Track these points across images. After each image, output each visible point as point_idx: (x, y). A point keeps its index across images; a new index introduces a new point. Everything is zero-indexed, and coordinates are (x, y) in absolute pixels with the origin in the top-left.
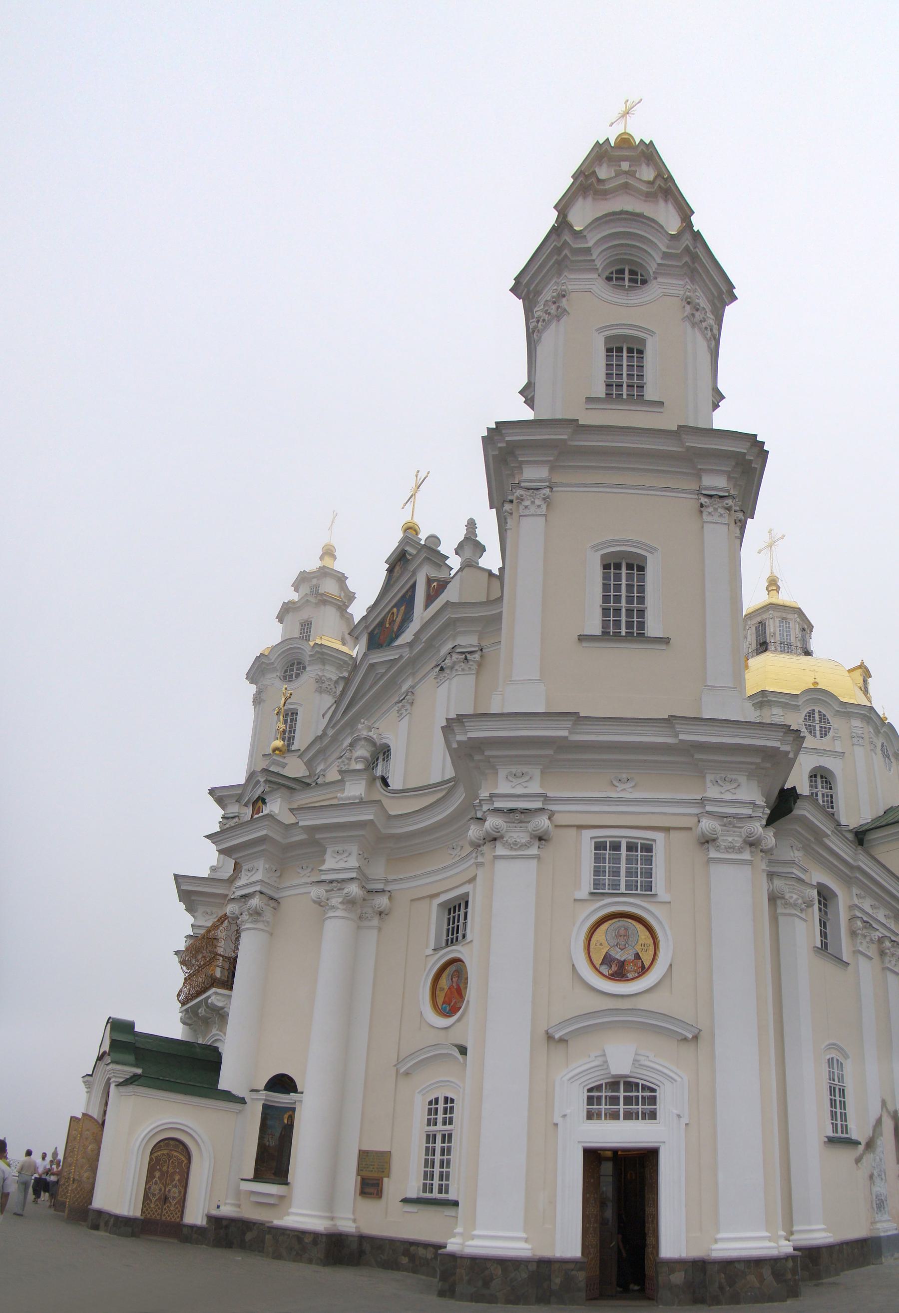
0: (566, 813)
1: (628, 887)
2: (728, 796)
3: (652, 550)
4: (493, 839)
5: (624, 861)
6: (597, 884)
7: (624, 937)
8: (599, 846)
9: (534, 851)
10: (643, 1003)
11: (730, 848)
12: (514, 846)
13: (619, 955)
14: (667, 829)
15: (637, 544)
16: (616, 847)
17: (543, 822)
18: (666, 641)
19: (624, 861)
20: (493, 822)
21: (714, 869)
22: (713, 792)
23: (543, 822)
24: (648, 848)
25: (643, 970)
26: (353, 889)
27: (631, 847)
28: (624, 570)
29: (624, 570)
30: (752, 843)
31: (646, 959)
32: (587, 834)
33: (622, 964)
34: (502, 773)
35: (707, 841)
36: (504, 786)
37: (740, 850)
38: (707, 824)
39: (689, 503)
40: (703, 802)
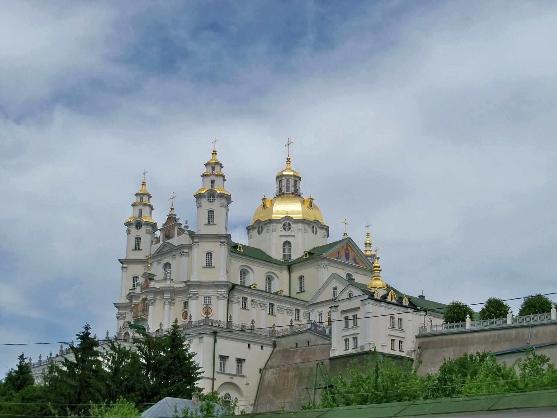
4: (191, 297)
5: (208, 300)
17: (197, 295)
19: (208, 300)
20: (191, 295)
23: (197, 295)
26: (170, 300)
28: (209, 255)
29: (209, 255)
35: (218, 297)
36: (193, 291)
39: (219, 243)
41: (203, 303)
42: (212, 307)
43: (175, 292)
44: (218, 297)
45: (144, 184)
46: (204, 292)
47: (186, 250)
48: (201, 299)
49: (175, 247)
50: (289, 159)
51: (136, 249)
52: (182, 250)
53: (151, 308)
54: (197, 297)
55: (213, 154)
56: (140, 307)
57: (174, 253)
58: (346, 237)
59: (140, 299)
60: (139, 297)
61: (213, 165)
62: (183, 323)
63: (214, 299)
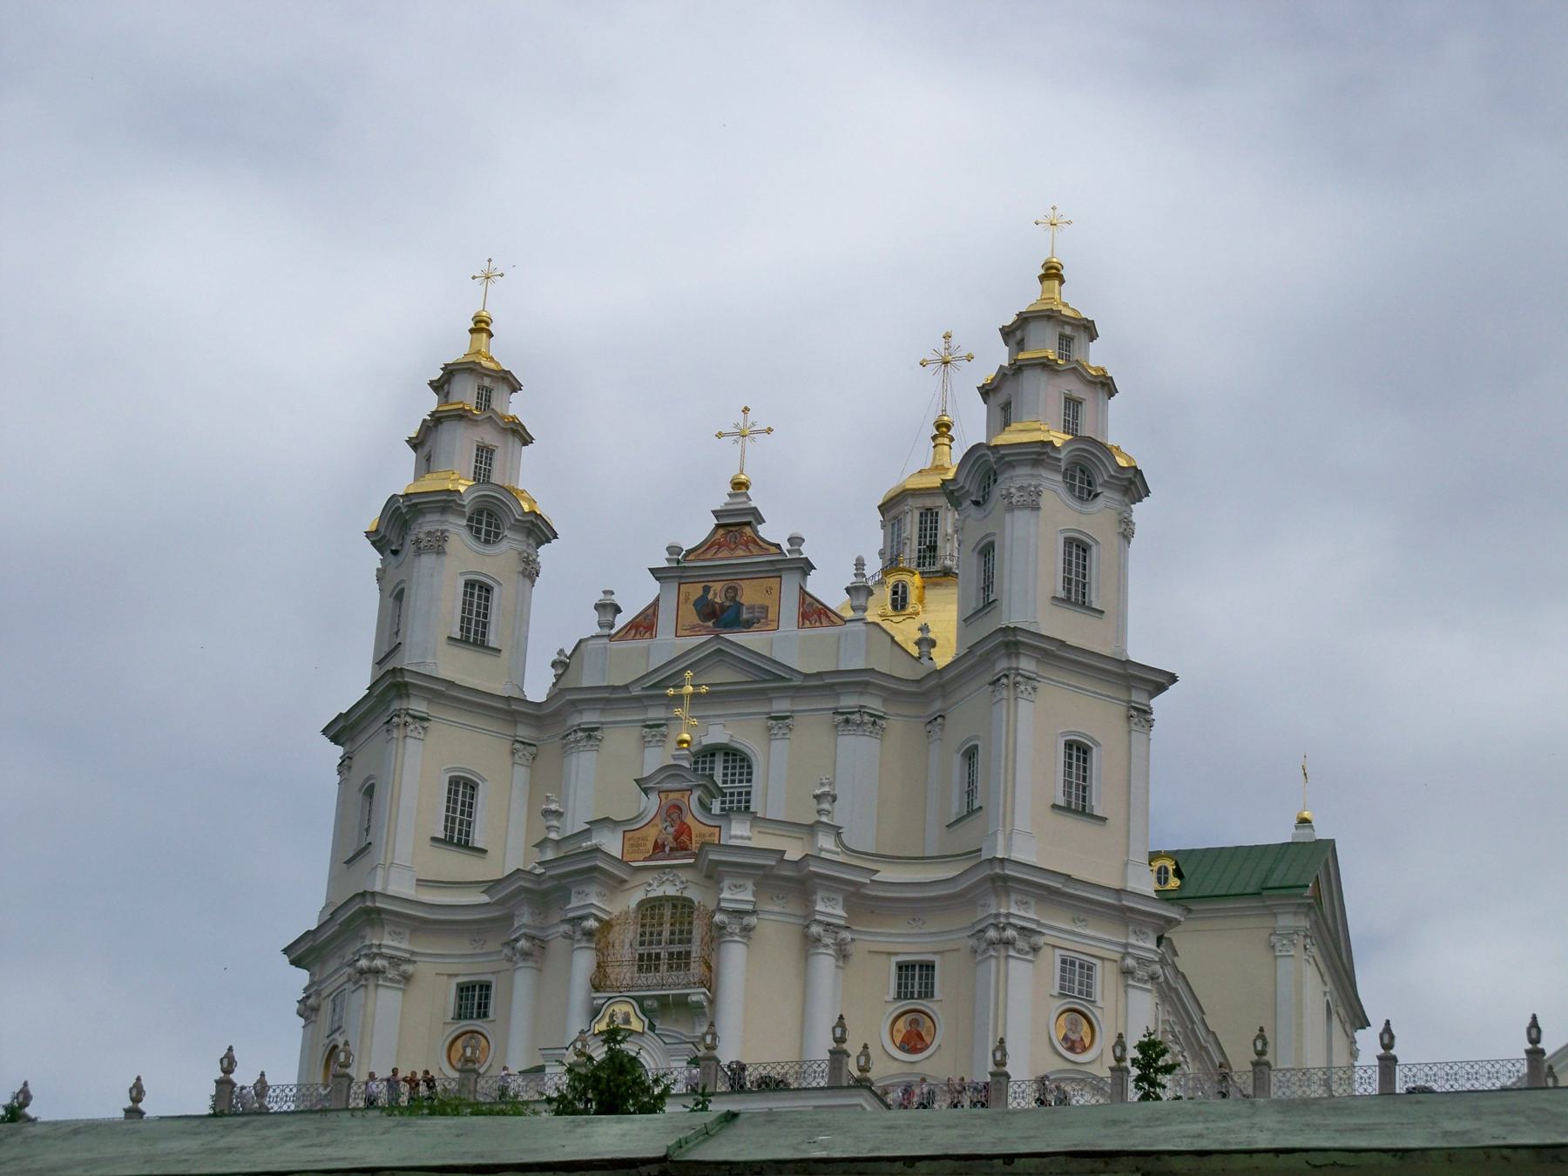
0: (1049, 938)
1: (1080, 992)
2: (1141, 944)
3: (1098, 744)
4: (1008, 943)
6: (1062, 988)
7: (1074, 1026)
8: (1064, 961)
9: (1029, 957)
10: (1088, 1069)
11: (1139, 980)
12: (1019, 951)
13: (1074, 1037)
14: (1102, 959)
15: (1084, 736)
16: (1073, 964)
18: (1104, 819)
19: (1076, 975)
20: (1010, 933)
21: (1131, 992)
22: (1133, 940)
24: (1090, 969)
25: (1085, 1049)
27: (1081, 966)
30: (1153, 978)
31: (1087, 1041)
32: (1058, 952)
33: (1073, 1042)
34: (1013, 897)
37: (1146, 982)
38: (1130, 962)
40: (1126, 946)
41: (1056, 991)
42: (1096, 1014)
43: (867, 903)
44: (1127, 973)
45: (481, 326)
46: (1064, 933)
47: (874, 704)
48: (1051, 962)
49: (806, 676)
50: (948, 427)
51: (463, 641)
52: (849, 701)
53: (735, 959)
54: (1035, 949)
55: (1043, 278)
56: (625, 943)
57: (781, 706)
58: (1304, 835)
59: (634, 898)
60: (617, 884)
61: (1068, 330)
62: (894, 1068)
63: (1105, 980)
